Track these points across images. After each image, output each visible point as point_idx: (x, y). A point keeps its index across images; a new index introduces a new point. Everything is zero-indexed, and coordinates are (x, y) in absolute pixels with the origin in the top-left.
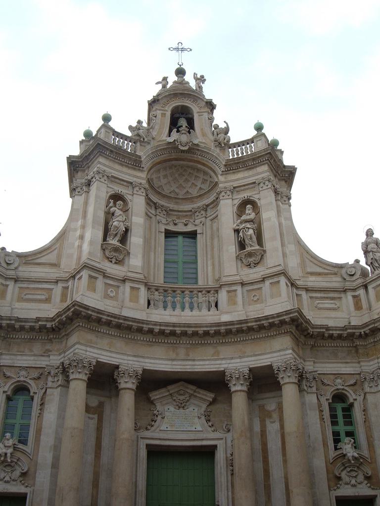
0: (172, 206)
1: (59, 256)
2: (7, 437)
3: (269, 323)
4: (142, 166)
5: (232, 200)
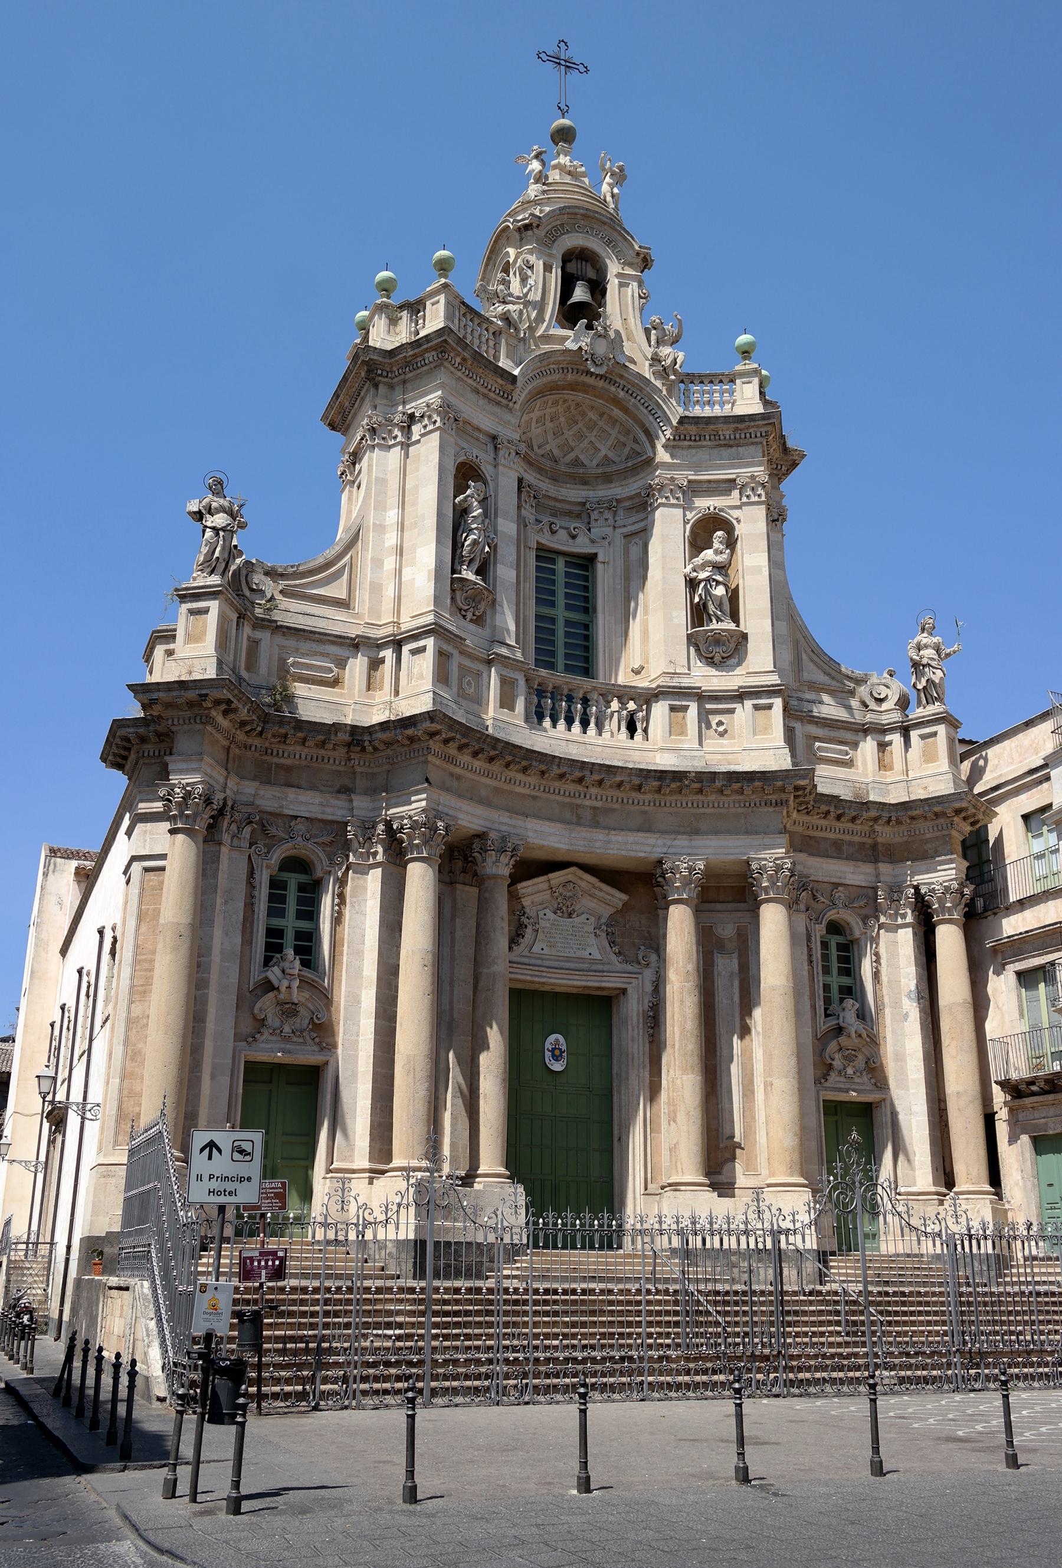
0: (545, 486)
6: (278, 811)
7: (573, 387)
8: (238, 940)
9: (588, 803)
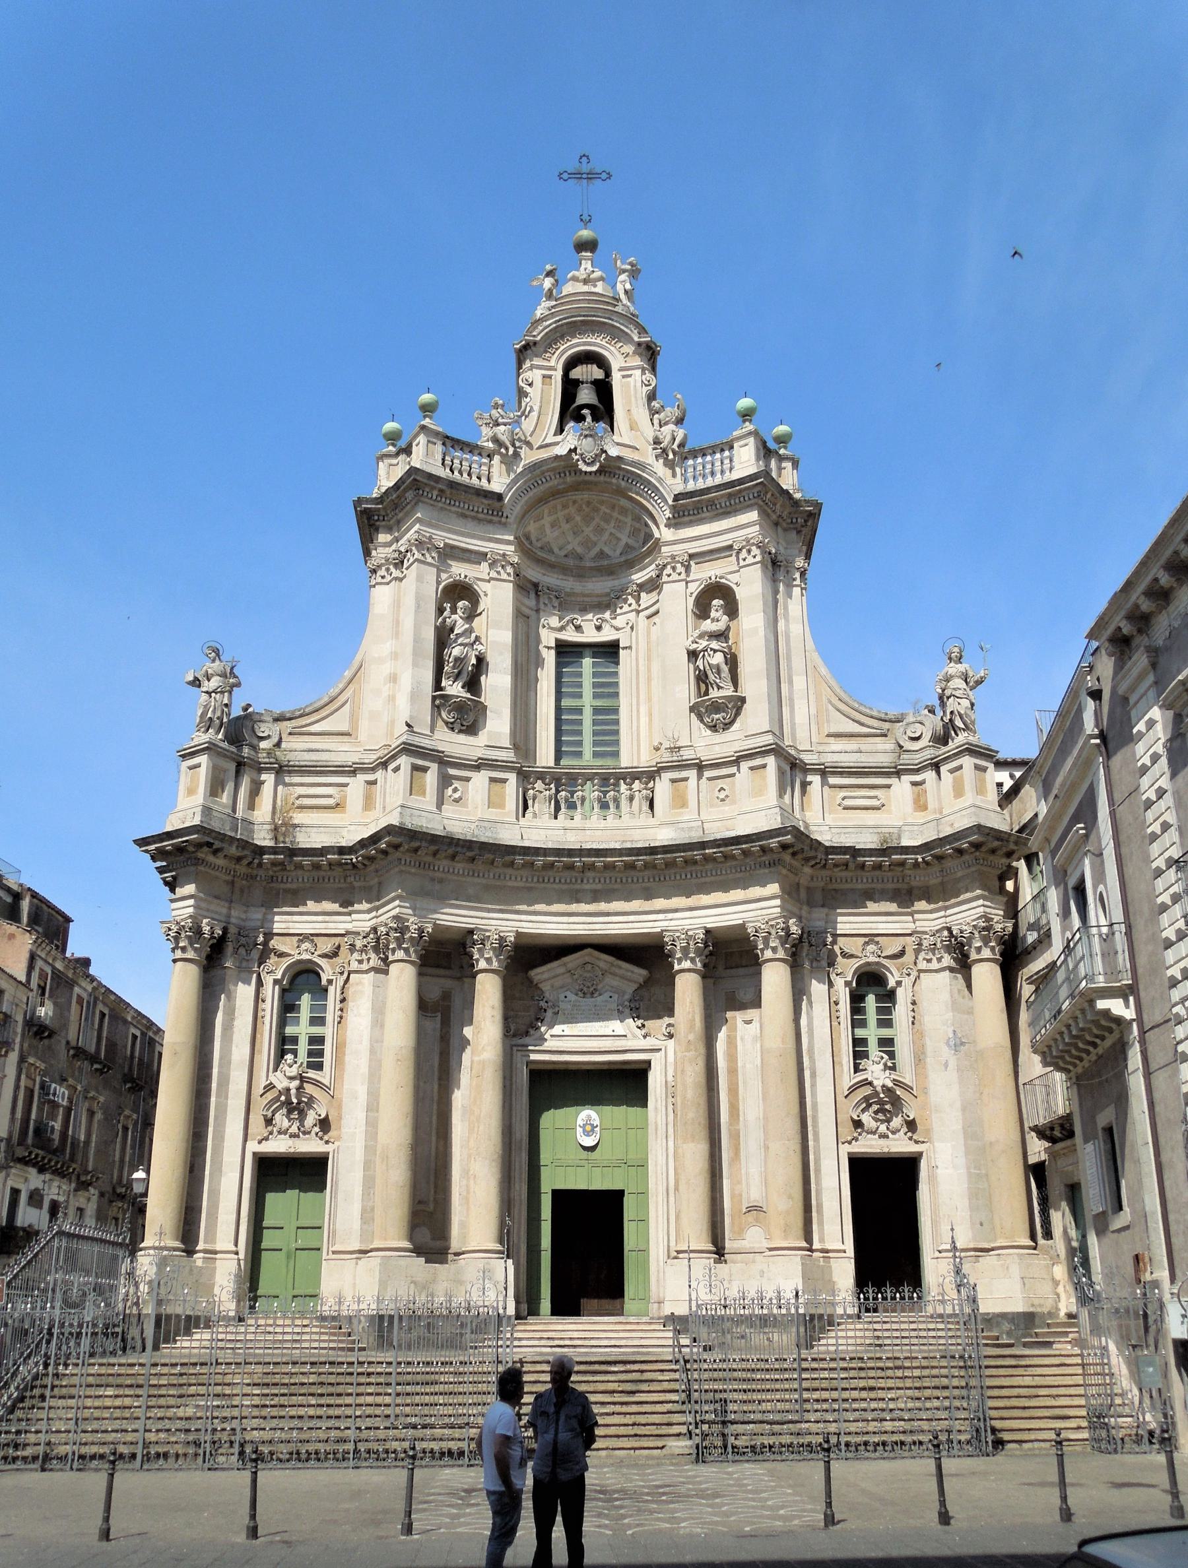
1: (354, 719)
2: (288, 1062)
5: (687, 583)
7: (576, 487)
9: (587, 887)
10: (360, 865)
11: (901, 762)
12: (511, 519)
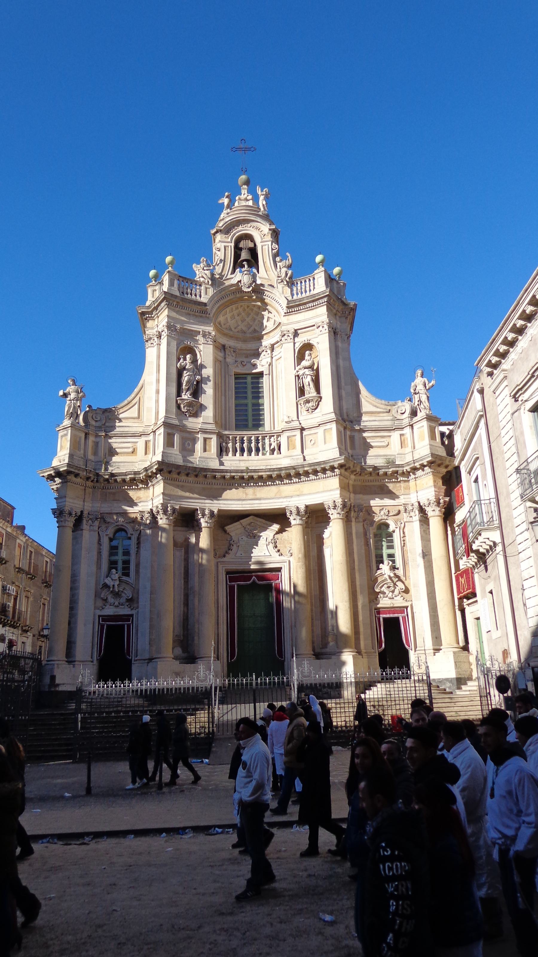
0: (239, 345)
3: (321, 468)
4: (208, 313)
6: (110, 512)
8: (94, 568)
10: (145, 481)
11: (395, 425)
12: (212, 315)
